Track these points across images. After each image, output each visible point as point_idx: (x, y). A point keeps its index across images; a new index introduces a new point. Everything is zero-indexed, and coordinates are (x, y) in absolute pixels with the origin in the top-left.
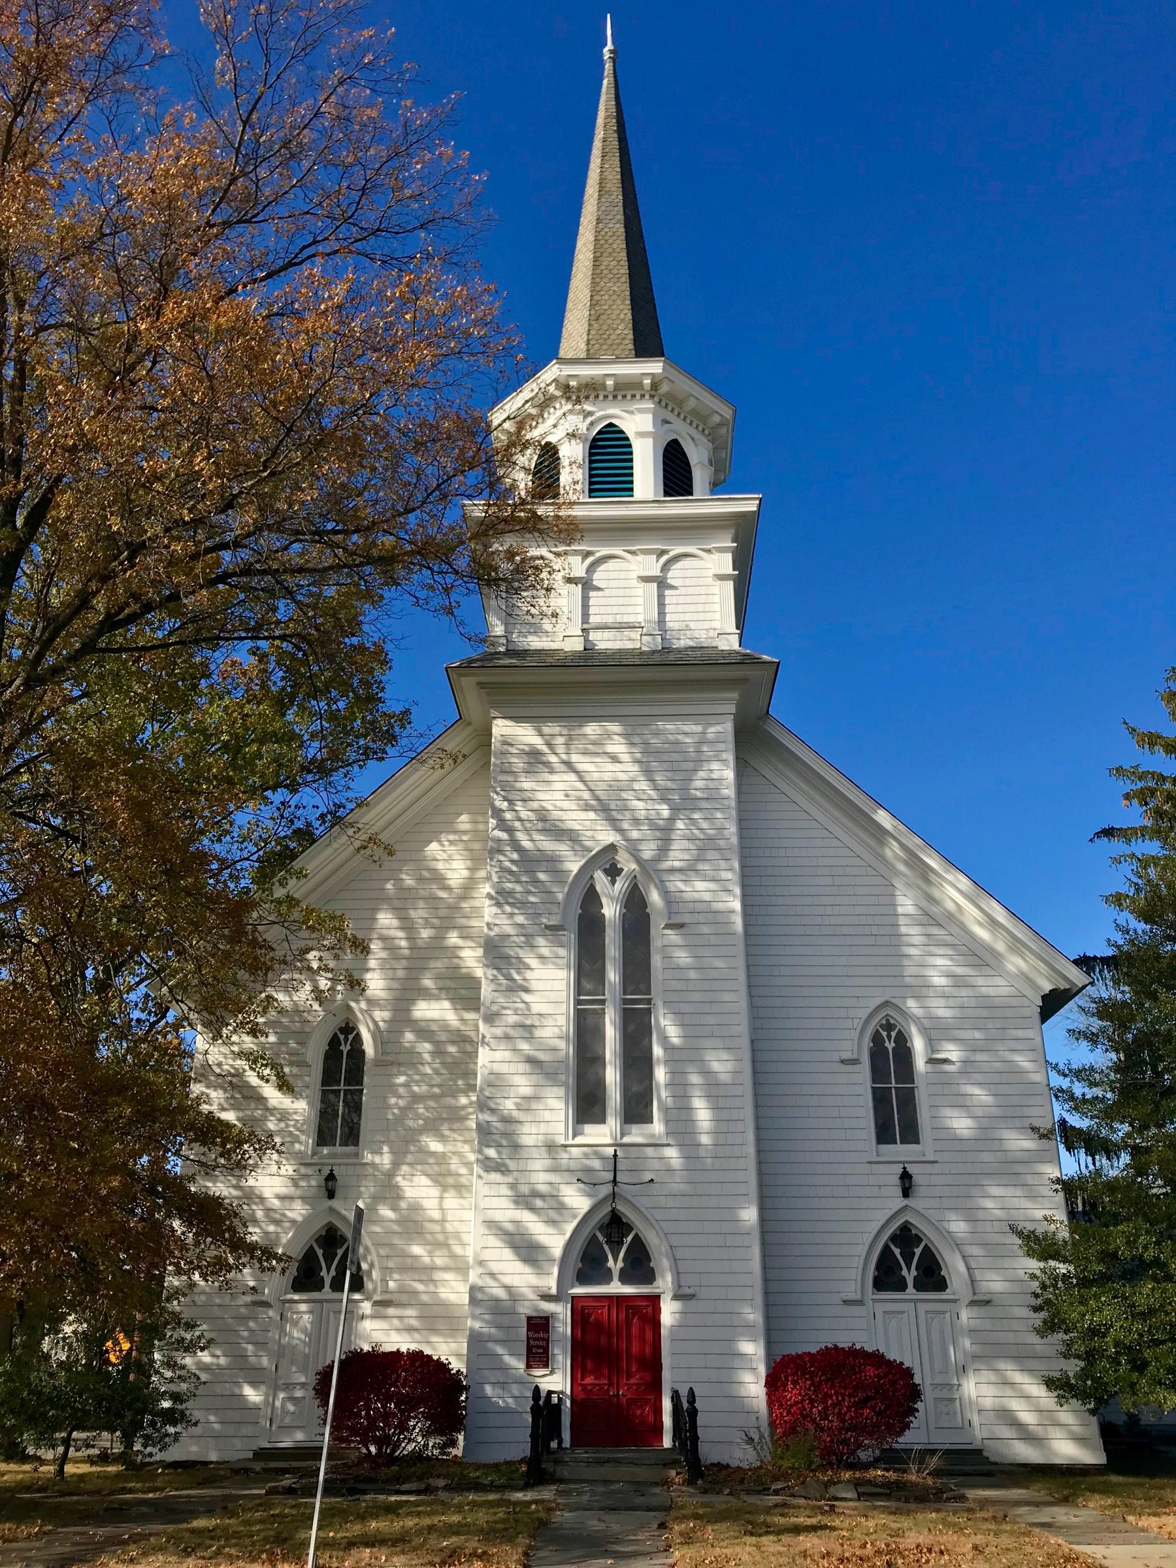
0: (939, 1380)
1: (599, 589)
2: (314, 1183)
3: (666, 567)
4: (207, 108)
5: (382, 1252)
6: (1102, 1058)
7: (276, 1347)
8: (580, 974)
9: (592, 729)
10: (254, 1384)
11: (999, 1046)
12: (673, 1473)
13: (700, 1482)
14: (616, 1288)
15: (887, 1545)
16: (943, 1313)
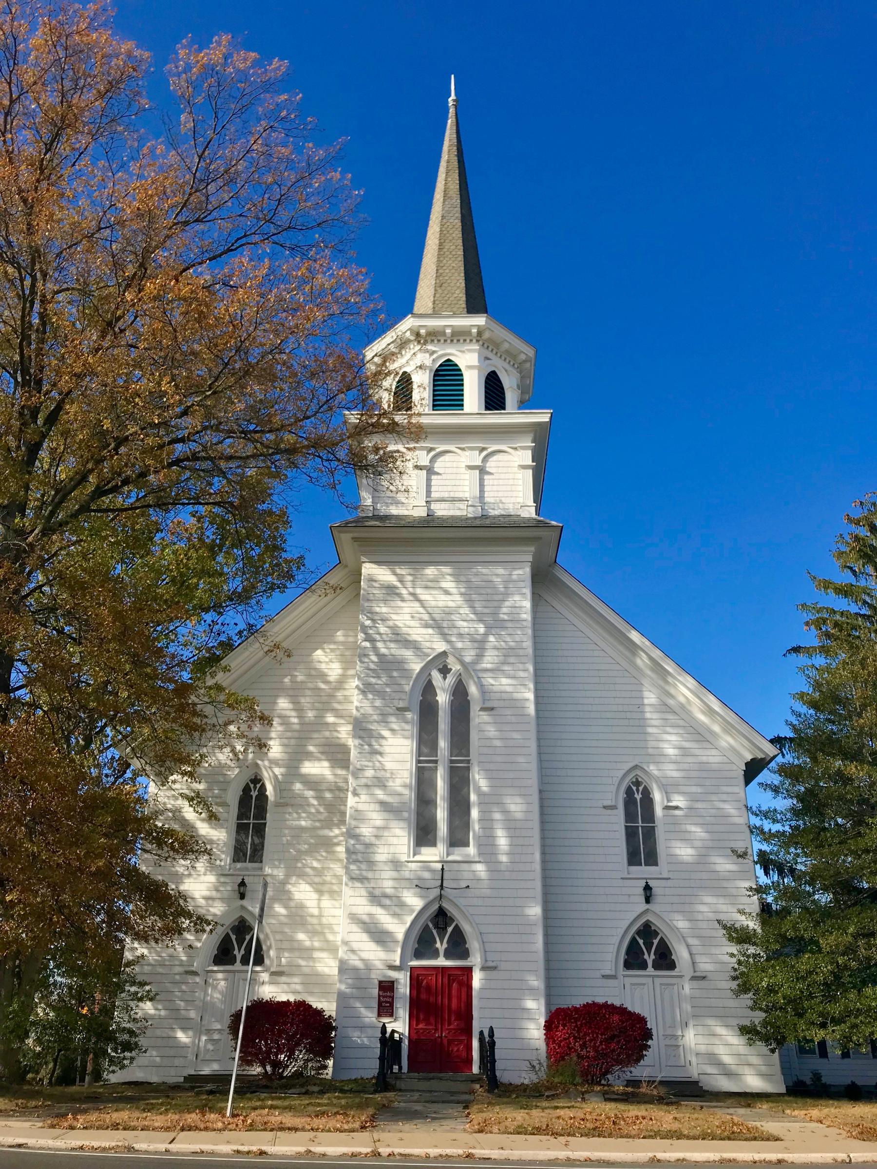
0: (669, 1032)
1: (438, 474)
2: (229, 888)
3: (485, 459)
4: (173, 144)
5: (278, 937)
6: (783, 804)
7: (201, 1004)
8: (421, 742)
9: (430, 571)
10: (184, 1029)
11: (714, 797)
12: (478, 1086)
13: (496, 1091)
14: (441, 962)
15: (616, 1115)
16: (674, 984)
